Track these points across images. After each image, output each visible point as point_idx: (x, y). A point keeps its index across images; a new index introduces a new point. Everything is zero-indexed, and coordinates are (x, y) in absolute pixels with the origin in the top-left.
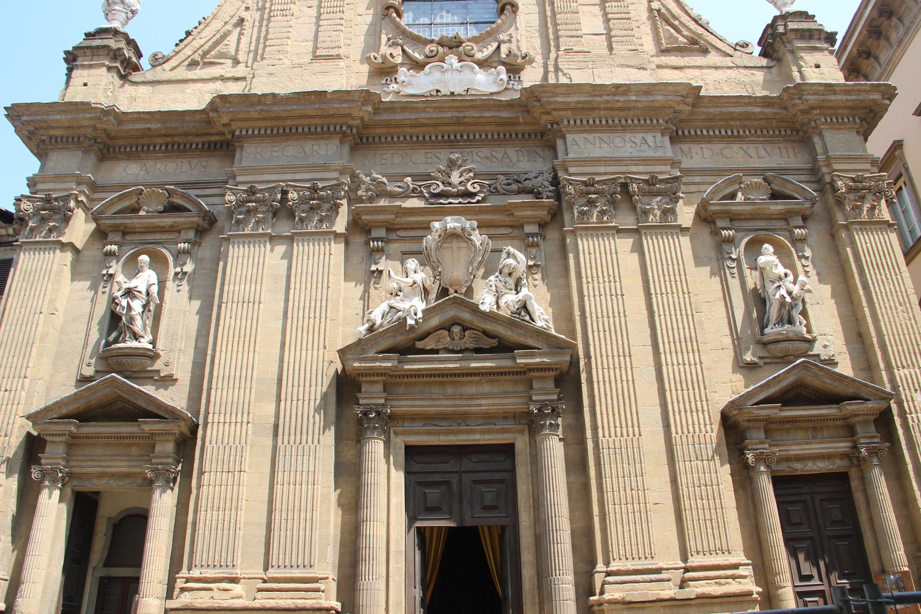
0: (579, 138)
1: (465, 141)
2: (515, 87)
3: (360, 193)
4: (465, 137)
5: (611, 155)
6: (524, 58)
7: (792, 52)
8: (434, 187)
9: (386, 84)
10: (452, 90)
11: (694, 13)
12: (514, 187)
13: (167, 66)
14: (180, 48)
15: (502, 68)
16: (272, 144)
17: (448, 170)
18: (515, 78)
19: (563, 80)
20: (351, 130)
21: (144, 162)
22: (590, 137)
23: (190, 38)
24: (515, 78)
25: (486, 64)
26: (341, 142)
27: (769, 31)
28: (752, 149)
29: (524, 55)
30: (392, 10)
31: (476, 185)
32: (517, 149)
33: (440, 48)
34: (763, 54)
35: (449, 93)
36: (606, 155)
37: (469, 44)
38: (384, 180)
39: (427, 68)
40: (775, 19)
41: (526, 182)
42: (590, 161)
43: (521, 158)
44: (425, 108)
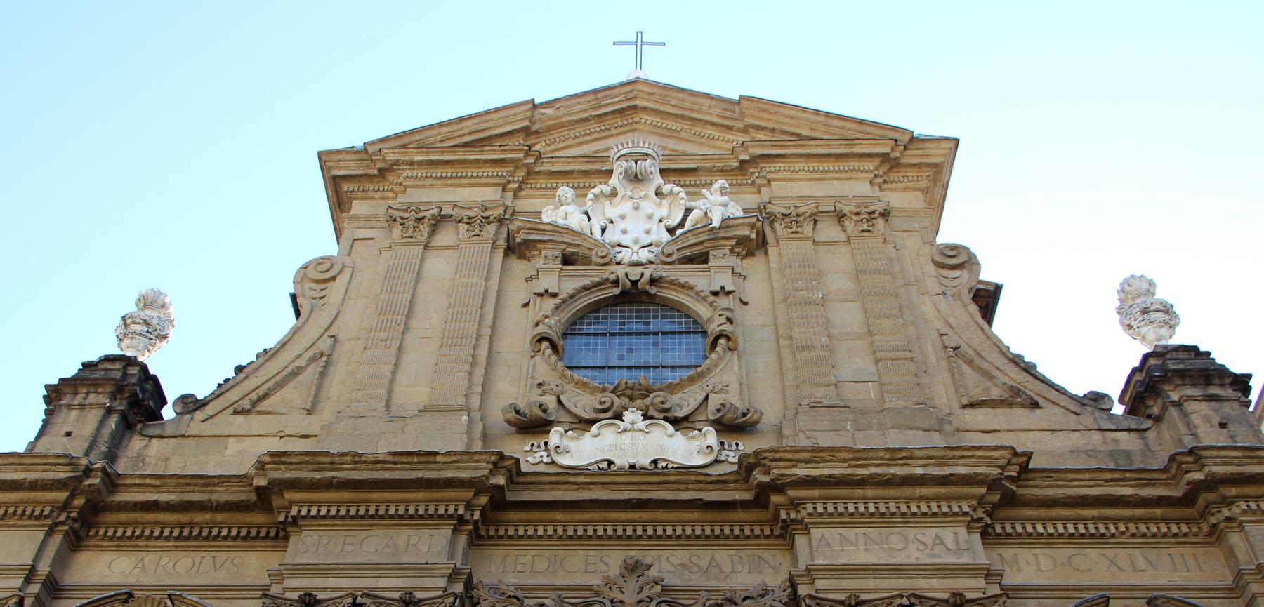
0: (832, 534)
1: (650, 537)
2: (730, 459)
5: (885, 562)
6: (744, 415)
7: (1178, 405)
10: (632, 461)
11: (1015, 350)
13: (199, 415)
14: (224, 388)
15: (710, 430)
16: (346, 533)
17: (621, 580)
18: (730, 446)
19: (804, 443)
20: (472, 515)
21: (141, 555)
22: (851, 533)
23: (242, 375)
24: (730, 446)
26: (456, 530)
27: (1138, 377)
28: (1122, 555)
30: (545, 344)
34: (1131, 411)
35: (627, 466)
36: (876, 561)
37: (661, 393)
38: (519, 594)
39: (594, 429)
40: (1146, 357)
42: (850, 570)
43: (739, 567)
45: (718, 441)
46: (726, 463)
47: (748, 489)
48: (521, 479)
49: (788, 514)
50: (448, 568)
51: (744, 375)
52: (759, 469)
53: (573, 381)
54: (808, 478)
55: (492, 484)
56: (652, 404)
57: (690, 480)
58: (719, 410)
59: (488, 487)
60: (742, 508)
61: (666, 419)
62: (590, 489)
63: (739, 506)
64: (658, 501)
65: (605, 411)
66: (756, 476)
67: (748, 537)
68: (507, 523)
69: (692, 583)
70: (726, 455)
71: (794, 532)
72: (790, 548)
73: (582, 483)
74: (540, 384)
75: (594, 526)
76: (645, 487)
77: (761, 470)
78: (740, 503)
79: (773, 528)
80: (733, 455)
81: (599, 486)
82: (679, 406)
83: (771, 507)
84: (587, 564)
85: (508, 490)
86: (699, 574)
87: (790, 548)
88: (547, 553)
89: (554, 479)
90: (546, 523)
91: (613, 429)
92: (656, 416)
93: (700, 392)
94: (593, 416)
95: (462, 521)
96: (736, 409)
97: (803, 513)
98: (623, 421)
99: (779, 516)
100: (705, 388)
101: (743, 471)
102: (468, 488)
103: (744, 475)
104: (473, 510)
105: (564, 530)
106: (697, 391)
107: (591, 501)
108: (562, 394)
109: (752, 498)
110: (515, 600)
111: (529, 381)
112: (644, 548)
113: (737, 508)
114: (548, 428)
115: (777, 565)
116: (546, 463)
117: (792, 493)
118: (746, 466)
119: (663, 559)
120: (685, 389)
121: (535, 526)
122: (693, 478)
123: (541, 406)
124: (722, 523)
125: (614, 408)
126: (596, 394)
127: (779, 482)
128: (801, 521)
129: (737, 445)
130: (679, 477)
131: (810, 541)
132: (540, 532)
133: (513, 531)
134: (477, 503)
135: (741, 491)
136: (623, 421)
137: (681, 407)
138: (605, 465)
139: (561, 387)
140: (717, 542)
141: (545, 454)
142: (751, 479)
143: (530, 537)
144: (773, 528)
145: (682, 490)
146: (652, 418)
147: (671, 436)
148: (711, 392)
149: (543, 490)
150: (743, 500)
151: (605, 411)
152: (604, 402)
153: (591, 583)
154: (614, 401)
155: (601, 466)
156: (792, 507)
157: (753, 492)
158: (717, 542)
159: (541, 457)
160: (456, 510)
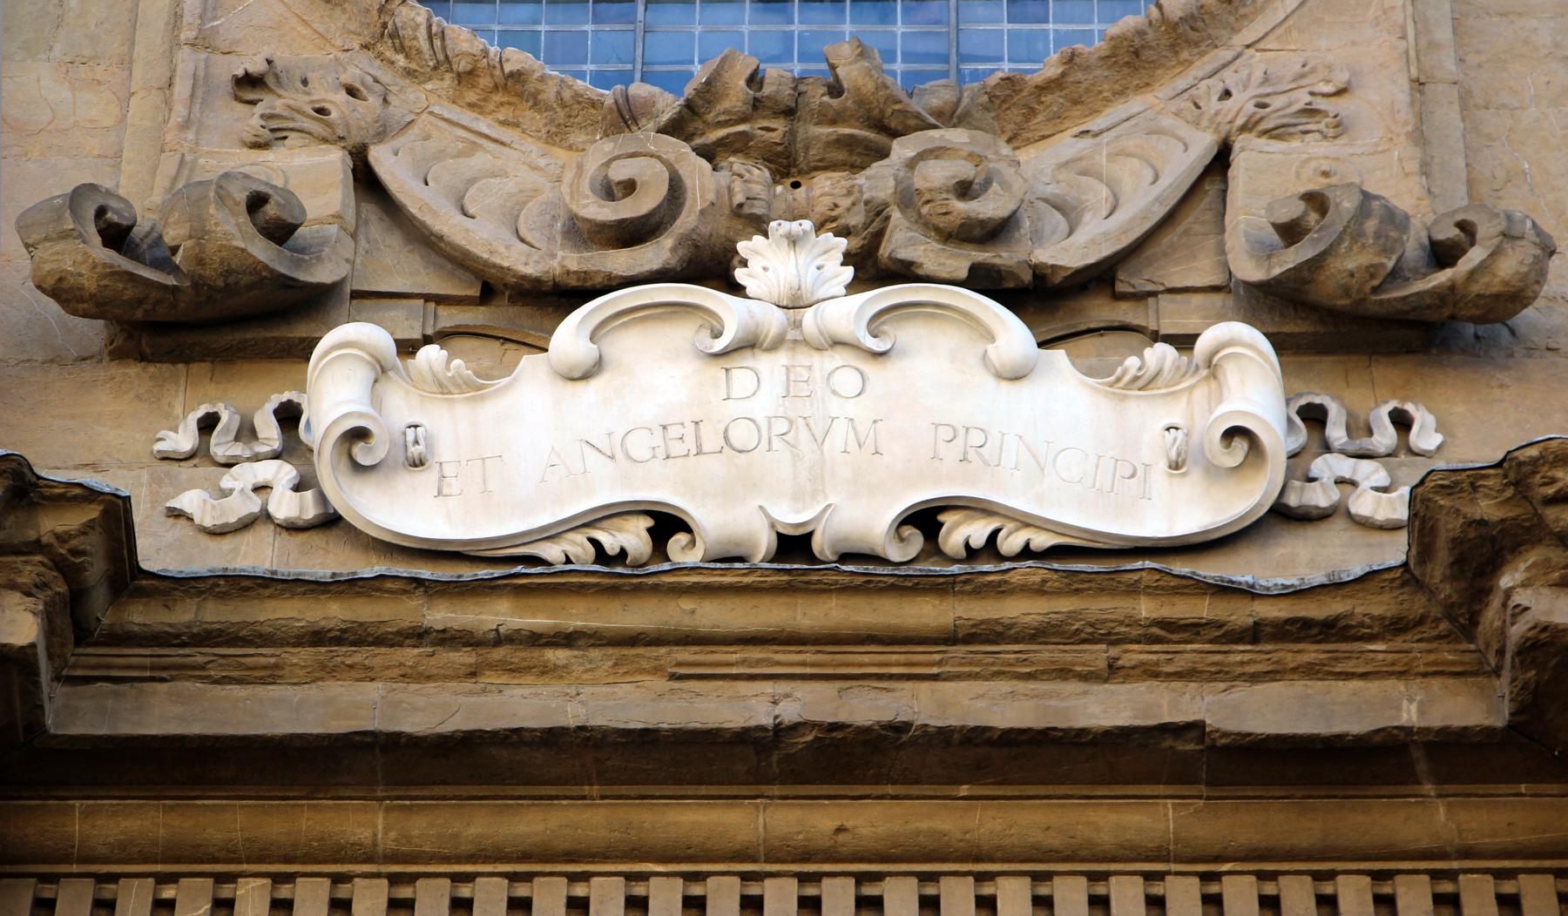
2: (1364, 504)
6: (1442, 254)
9: (199, 454)
10: (791, 516)
18: (1360, 427)
24: (1360, 427)
25: (1101, 311)
29: (1449, 232)
33: (696, 170)
35: (764, 543)
37: (957, 136)
44: (536, 640)
45: (1288, 402)
46: (1338, 524)
48: (140, 616)
51: (1444, 34)
52: (1533, 556)
53: (444, 63)
56: (907, 198)
57: (1133, 622)
58: (1291, 232)
61: (983, 281)
62: (546, 671)
63: (1422, 767)
64: (945, 736)
65: (632, 234)
66: (1521, 598)
70: (1340, 482)
74: (249, 83)
76: (865, 659)
77: (1546, 566)
80: (1382, 478)
81: (595, 653)
82: (1059, 206)
85: (57, 678)
89: (335, 612)
91: (682, 333)
92: (929, 265)
93: (1185, 131)
94: (565, 261)
96: (1395, 220)
98: (737, 289)
100: (1212, 105)
101: (1437, 571)
103: (1446, 591)
106: (1167, 121)
107: (553, 739)
108: (382, 135)
109: (1499, 721)
111: (187, 61)
113: (1411, 778)
114: (300, 331)
116: (292, 528)
118: (1455, 542)
120: (1095, 112)
121: (221, 879)
122: (1146, 609)
123: (256, 202)
125: (687, 221)
126: (578, 138)
129: (1402, 422)
130: (1065, 605)
135: (1436, 684)
136: (737, 289)
137: (1069, 212)
138: (633, 537)
139: (373, 101)
141: (282, 474)
142: (1491, 616)
145: (1085, 677)
146: (905, 273)
147: (1016, 376)
148: (1244, 128)
149: (272, 675)
150: (1444, 731)
151: (632, 234)
152: (629, 187)
154: (683, 172)
155: (611, 543)
157: (1503, 685)
159: (261, 488)
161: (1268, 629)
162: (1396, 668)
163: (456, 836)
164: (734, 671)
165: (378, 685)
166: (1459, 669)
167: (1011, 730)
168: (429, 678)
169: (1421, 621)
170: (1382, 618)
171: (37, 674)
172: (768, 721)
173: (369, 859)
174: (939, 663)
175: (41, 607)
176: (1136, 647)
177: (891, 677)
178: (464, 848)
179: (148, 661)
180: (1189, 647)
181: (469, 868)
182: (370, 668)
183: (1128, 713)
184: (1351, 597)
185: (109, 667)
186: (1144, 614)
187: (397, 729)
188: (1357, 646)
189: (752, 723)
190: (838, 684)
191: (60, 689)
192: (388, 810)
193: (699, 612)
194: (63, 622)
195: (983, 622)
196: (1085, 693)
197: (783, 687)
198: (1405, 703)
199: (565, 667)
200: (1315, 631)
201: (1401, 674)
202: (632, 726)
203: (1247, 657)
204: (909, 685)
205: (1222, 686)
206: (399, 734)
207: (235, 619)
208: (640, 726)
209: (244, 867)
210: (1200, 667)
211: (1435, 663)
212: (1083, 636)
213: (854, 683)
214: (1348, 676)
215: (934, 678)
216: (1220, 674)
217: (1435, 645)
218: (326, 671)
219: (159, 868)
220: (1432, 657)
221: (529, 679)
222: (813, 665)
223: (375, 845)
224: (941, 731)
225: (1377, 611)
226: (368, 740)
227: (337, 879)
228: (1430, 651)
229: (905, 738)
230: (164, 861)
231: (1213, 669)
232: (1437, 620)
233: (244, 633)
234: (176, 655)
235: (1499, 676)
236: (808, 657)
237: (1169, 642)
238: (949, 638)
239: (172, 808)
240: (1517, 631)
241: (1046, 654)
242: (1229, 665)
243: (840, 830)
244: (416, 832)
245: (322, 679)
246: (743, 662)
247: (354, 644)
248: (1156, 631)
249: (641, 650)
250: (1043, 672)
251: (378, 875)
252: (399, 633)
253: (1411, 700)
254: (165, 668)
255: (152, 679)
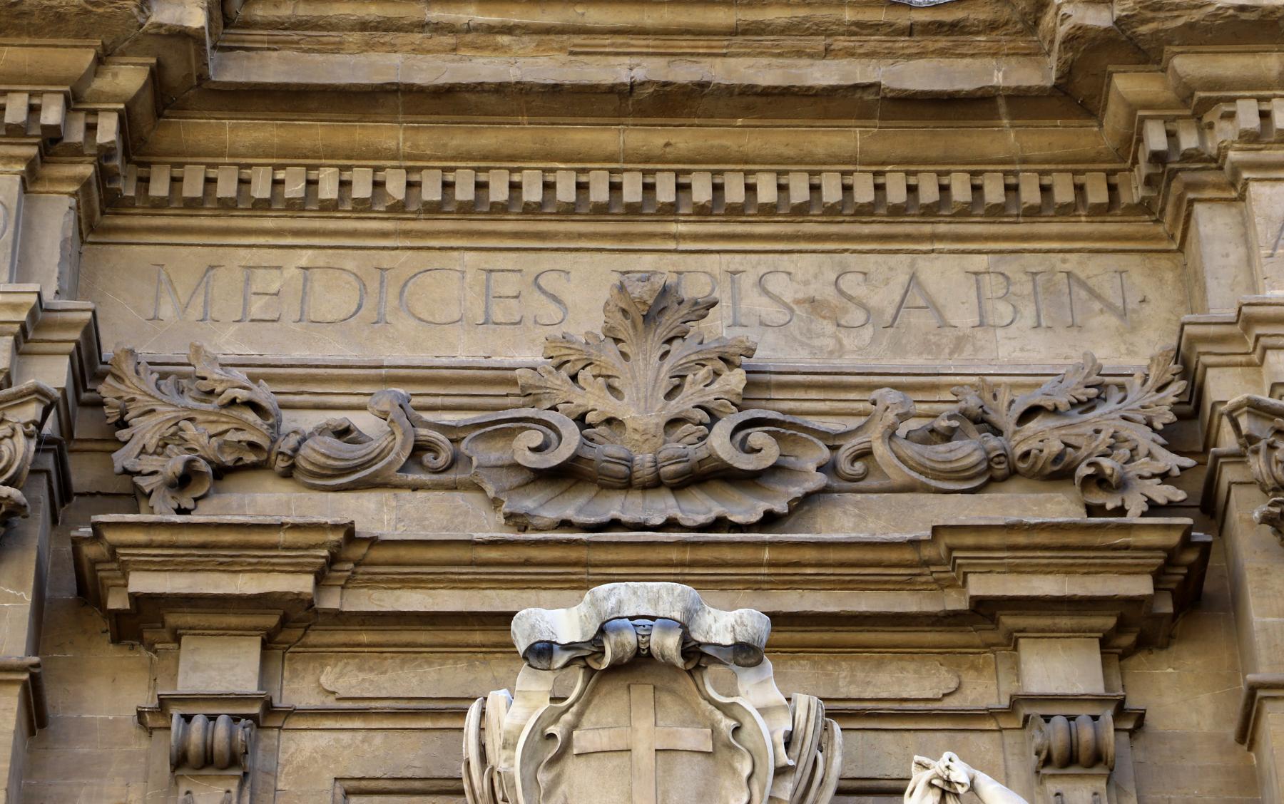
1: (702, 212)
3: (124, 458)
4: (701, 192)
8: (535, 437)
12: (967, 450)
20: (91, 128)
31: (757, 437)
32: (980, 262)
38: (263, 394)
41: (1033, 425)
43: (1005, 310)
44: (491, 30)
47: (1033, 54)
49: (1171, 135)
50: (15, 307)
54: (1244, 16)
55: (160, 26)
57: (840, 23)
59: (146, 34)
60: (1013, 116)
62: (497, 48)
63: (1003, 110)
64: (729, 91)
66: (1066, 9)
67: (1032, 213)
68: (212, 156)
69: (845, 363)
71: (1191, 195)
72: (1174, 247)
73: (469, 29)
75: (512, 171)
76: (684, 44)
78: (1008, 98)
79: (1117, 179)
81: (526, 38)
83: (1114, 116)
84: (489, 295)
85: (214, 47)
86: (868, 333)
87: (1174, 247)
88: (350, 261)
90: (346, 158)
95: (52, 144)
97: (1224, 133)
99: (1140, 140)
102: (76, 36)
104: (95, 112)
105: (410, 185)
107: (500, 89)
110: (251, 416)
112: (683, 246)
113: (994, 115)
115: (1132, 303)
117: (1188, 65)
119: (747, 281)
124: (943, 165)
127: (1144, 29)
128: (1216, 161)
131: (1245, 224)
132: (328, 190)
133: (234, 185)
134: (107, 89)
135: (1013, 60)
140: (927, 229)
142: (1048, 20)
143: (294, 207)
144: (1117, 179)
145: (811, 56)
149: (337, 48)
150: (1017, 88)
153: (507, 362)
156: (1188, 112)
157: (1052, 62)
158: (927, 229)
160: (34, 110)
161: (919, 28)
162: (991, 51)
163: (445, 145)
164: (607, 50)
165: (399, 55)
166: (1028, 52)
167: (768, 87)
168: (429, 51)
169: (1006, 23)
170: (985, 21)
171: (205, 45)
172: (627, 80)
173: (394, 158)
174: (727, 47)
175: (206, 5)
176: (842, 38)
177: (699, 54)
178: (450, 152)
179: (266, 38)
180: (873, 38)
181: (452, 164)
182: (393, 45)
183: (836, 77)
184: (968, 8)
185: (243, 41)
186: (847, 18)
187: (411, 82)
188: (969, 37)
189: (618, 81)
190: (668, 59)
191: (216, 54)
192: (406, 129)
193: (587, 14)
194: (217, 14)
195: (753, 22)
196: (812, 65)
197: (635, 60)
198: (996, 72)
199: (508, 46)
200: (946, 29)
201: (994, 55)
202: (548, 82)
203: (906, 44)
204: (709, 60)
205: (891, 61)
206: (413, 85)
207: (316, 14)
208: (553, 82)
209: (323, 161)
210: (878, 50)
211: (1014, 48)
212: (811, 31)
213: (677, 58)
214: (963, 56)
215: (724, 55)
216: (891, 54)
217: (1014, 37)
218: (369, 46)
219: (274, 161)
220: (1012, 45)
221: (487, 53)
222: (653, 47)
223: (398, 149)
224: (728, 87)
225: (982, 17)
226: (395, 88)
227: (747, 173)
228: (1011, 41)
229: (706, 91)
230: (278, 157)
231: (886, 51)
232: (1016, 23)
233: (321, 22)
234: (282, 35)
235: (1049, 56)
236: (651, 42)
237: (861, 35)
238: (734, 32)
239: (281, 126)
240: (1062, 30)
241: (789, 42)
242: (896, 49)
243: (667, 145)
244: (422, 143)
245: (366, 51)
246: (612, 45)
247: (385, 30)
248: (854, 28)
249: (552, 37)
250: (787, 53)
251: (400, 167)
252: (411, 24)
253: (999, 70)
254: (276, 43)
255: (269, 49)
